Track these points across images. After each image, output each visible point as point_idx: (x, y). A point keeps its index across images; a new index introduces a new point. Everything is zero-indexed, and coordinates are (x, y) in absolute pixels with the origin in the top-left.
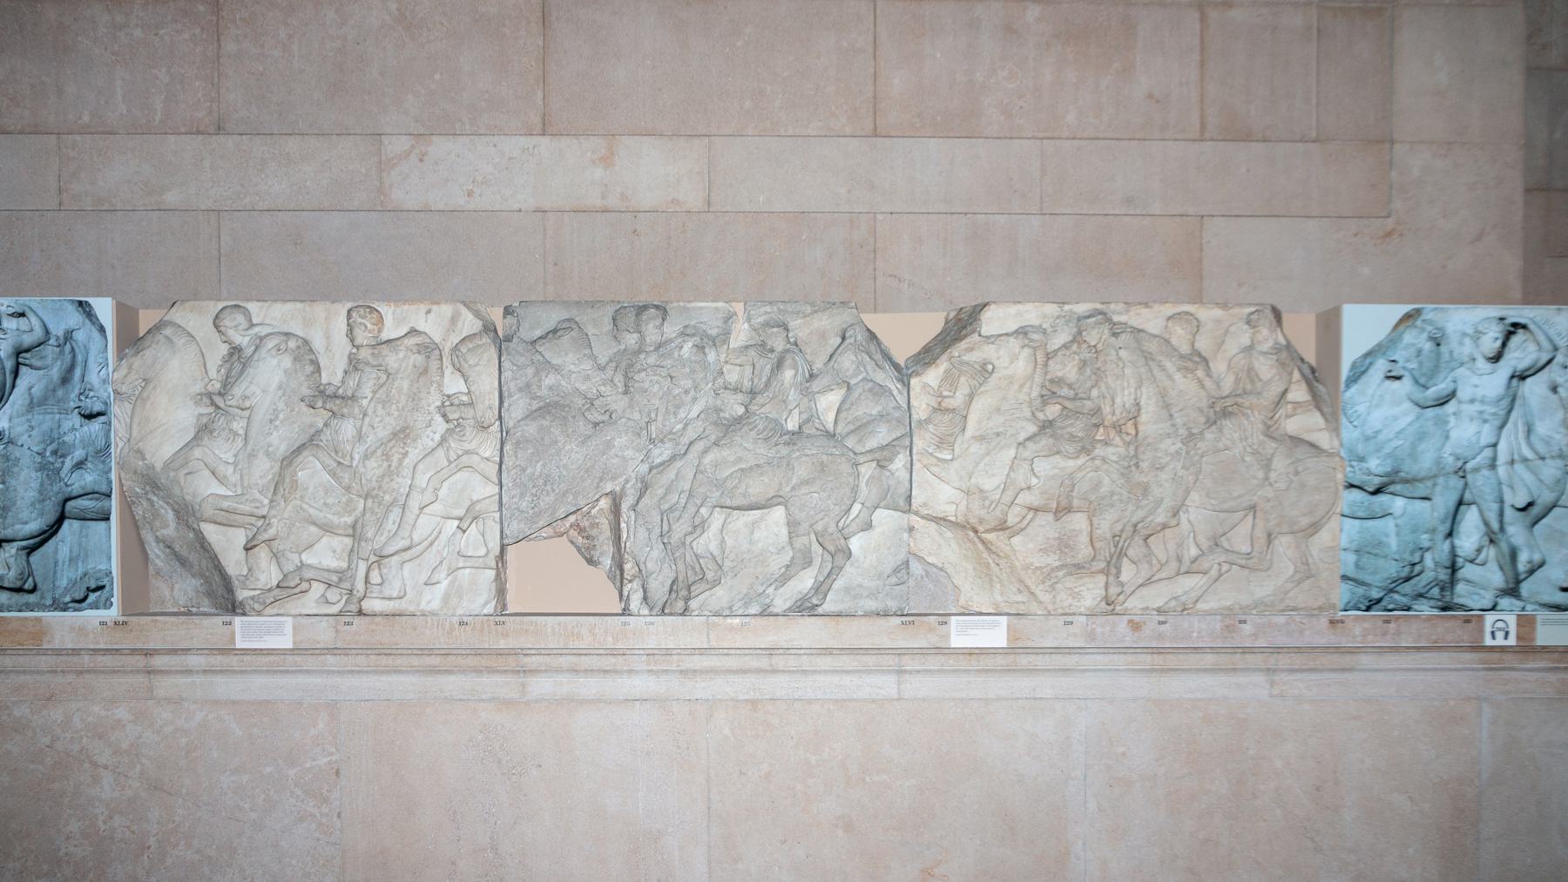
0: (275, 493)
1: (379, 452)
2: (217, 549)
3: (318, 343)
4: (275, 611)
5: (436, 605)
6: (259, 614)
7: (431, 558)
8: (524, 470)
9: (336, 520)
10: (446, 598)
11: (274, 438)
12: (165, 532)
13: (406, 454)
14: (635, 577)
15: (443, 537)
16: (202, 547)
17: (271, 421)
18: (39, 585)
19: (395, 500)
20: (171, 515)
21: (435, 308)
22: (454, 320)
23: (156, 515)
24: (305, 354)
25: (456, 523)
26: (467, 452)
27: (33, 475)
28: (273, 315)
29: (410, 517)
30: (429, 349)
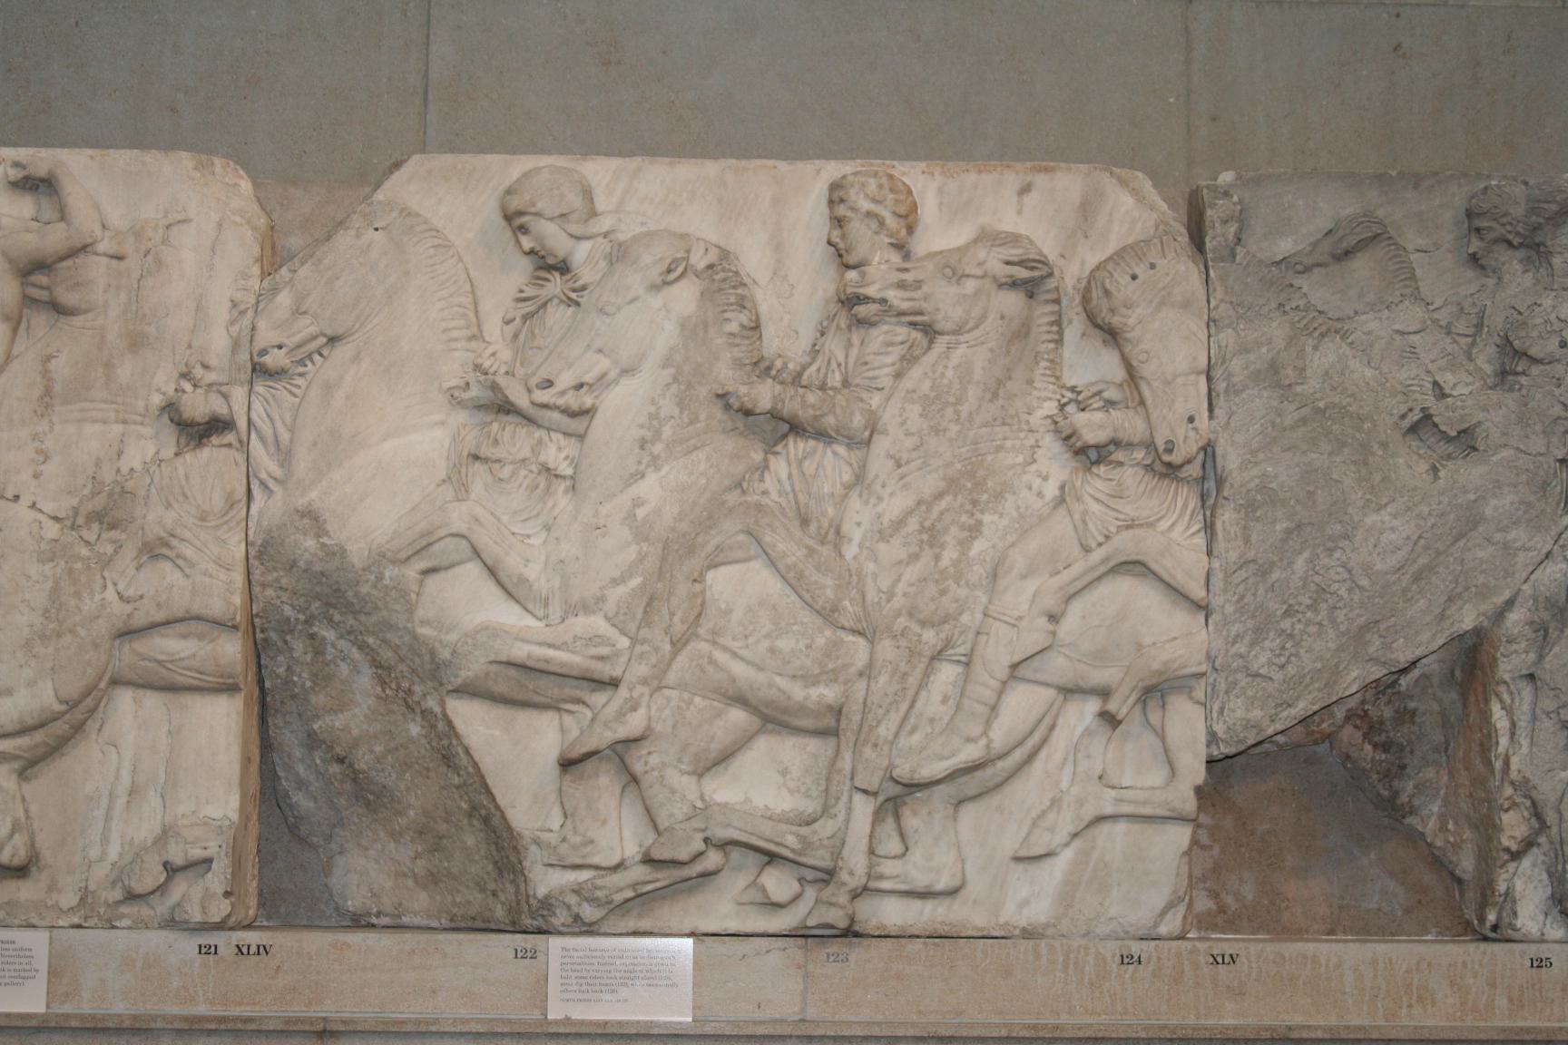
0: (647, 620)
1: (913, 525)
2: (487, 764)
3: (754, 260)
4: (632, 924)
5: (1039, 911)
6: (590, 929)
7: (1029, 792)
8: (1264, 573)
9: (798, 692)
10: (1067, 896)
11: (649, 487)
12: (339, 721)
13: (975, 530)
14: (1529, 844)
15: (1061, 740)
16: (447, 759)
17: (643, 444)
18: (46, 854)
19: (948, 643)
20: (365, 680)
21: (1041, 180)
22: (1087, 210)
23: (323, 677)
24: (722, 279)
25: (1092, 706)
26: (1130, 525)
27: (33, 569)
28: (644, 196)
29: (983, 688)
30: (1031, 280)
